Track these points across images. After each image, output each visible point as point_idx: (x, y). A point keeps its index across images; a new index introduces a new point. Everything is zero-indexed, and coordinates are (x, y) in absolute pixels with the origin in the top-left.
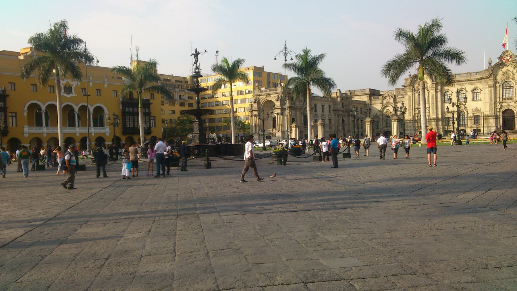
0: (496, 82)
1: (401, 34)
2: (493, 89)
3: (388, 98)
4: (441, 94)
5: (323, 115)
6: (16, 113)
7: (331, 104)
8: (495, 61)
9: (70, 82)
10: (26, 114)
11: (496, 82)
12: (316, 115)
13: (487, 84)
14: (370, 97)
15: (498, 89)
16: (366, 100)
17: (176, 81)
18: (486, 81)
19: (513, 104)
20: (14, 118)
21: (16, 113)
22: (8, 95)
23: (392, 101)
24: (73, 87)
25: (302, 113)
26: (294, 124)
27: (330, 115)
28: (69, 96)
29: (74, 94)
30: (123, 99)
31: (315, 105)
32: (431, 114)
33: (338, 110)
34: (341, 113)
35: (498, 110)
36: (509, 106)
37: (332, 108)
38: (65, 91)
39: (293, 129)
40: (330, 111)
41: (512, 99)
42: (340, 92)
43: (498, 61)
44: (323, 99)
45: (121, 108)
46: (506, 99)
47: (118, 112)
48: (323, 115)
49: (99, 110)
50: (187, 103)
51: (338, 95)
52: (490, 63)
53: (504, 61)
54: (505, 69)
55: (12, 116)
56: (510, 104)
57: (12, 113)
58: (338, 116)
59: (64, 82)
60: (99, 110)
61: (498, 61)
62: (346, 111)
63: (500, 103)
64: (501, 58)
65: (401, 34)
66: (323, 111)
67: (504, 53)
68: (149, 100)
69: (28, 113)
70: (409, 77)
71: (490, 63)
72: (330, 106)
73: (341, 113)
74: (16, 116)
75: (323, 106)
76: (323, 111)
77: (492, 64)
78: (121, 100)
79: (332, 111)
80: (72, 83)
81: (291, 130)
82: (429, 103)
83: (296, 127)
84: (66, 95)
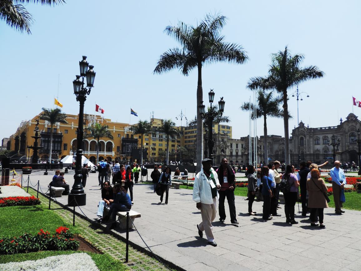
1: (43, 109)
5: (237, 149)
8: (344, 120)
10: (71, 145)
30: (123, 138)
31: (231, 144)
32: (307, 151)
36: (353, 148)
37: (244, 146)
43: (346, 120)
45: (122, 143)
47: (119, 145)
48: (237, 149)
49: (109, 144)
52: (341, 120)
53: (350, 120)
54: (350, 125)
56: (355, 147)
60: (109, 144)
61: (346, 120)
64: (348, 118)
65: (43, 109)
66: (237, 147)
68: (137, 139)
69: (73, 144)
72: (242, 145)
75: (237, 145)
76: (237, 147)
77: (343, 122)
78: (122, 139)
82: (306, 145)
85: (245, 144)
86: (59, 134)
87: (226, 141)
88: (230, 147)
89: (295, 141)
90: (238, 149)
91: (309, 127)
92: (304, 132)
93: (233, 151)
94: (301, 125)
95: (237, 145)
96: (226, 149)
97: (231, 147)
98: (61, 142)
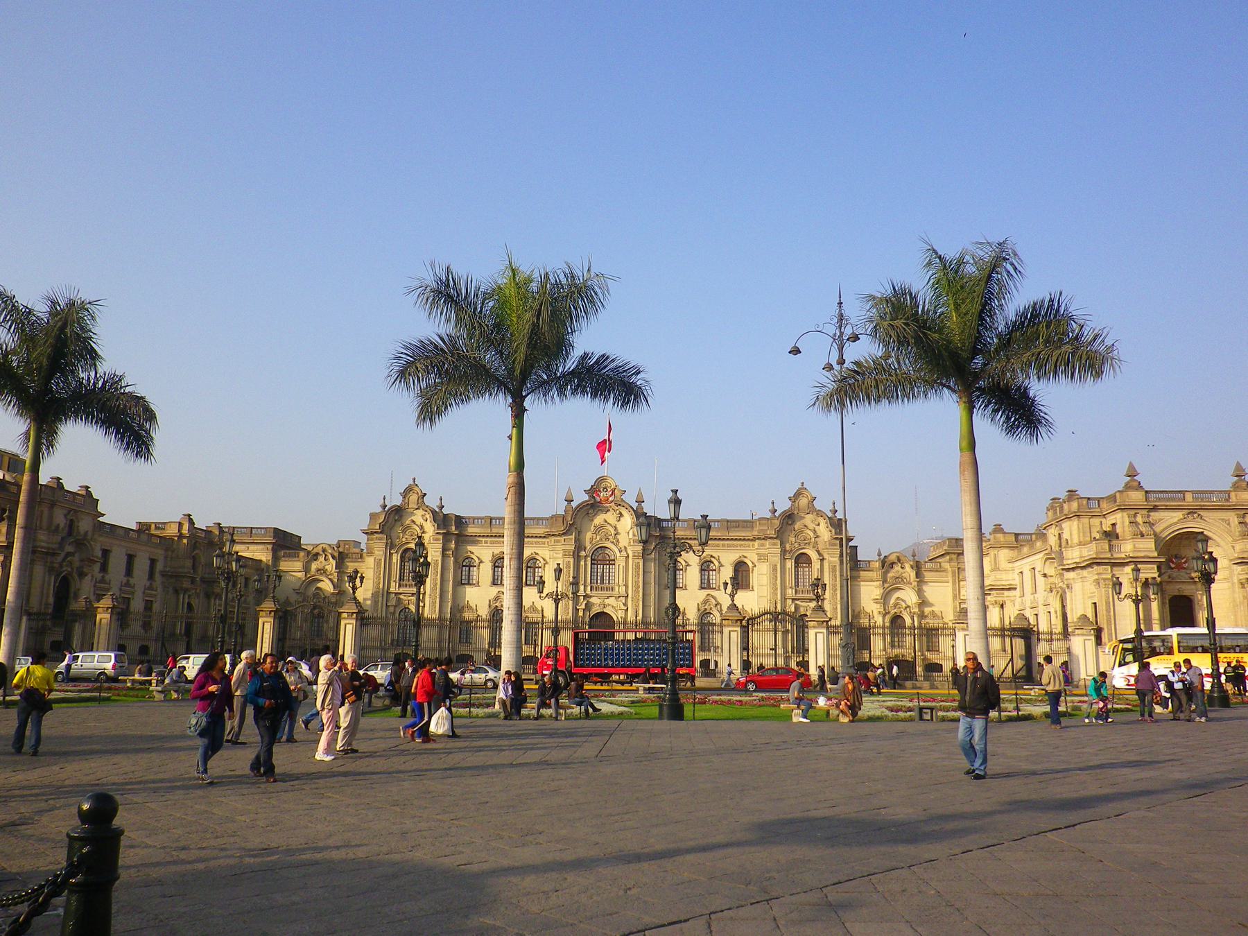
0: (579, 546)
2: (572, 561)
3: (321, 559)
4: (456, 561)
5: (127, 584)
7: (159, 554)
8: (580, 498)
11: (579, 546)
12: (103, 581)
13: (558, 548)
14: (274, 551)
15: (582, 563)
16: (264, 559)
18: (558, 541)
19: (612, 601)
23: (331, 566)
25: (51, 570)
27: (151, 588)
31: (106, 553)
33: (177, 576)
34: (186, 584)
35: (581, 614)
37: (159, 566)
40: (151, 576)
41: (612, 589)
42: (191, 522)
43: (586, 497)
44: (135, 535)
46: (598, 589)
48: (127, 584)
51: (185, 530)
52: (570, 501)
56: (607, 601)
58: (176, 592)
61: (586, 497)
62: (203, 580)
63: (586, 596)
64: (593, 491)
66: (129, 572)
67: (600, 480)
70: (380, 509)
71: (570, 501)
72: (153, 562)
73: (186, 584)
75: (130, 558)
76: (129, 572)
77: (574, 504)
79: (158, 577)
85: (166, 557)
87: (86, 533)
88: (97, 567)
89: (378, 563)
90: (132, 581)
91: (445, 511)
92: (422, 527)
93: (133, 593)
94: (413, 498)
95: (130, 558)
96: (82, 575)
97: (104, 568)
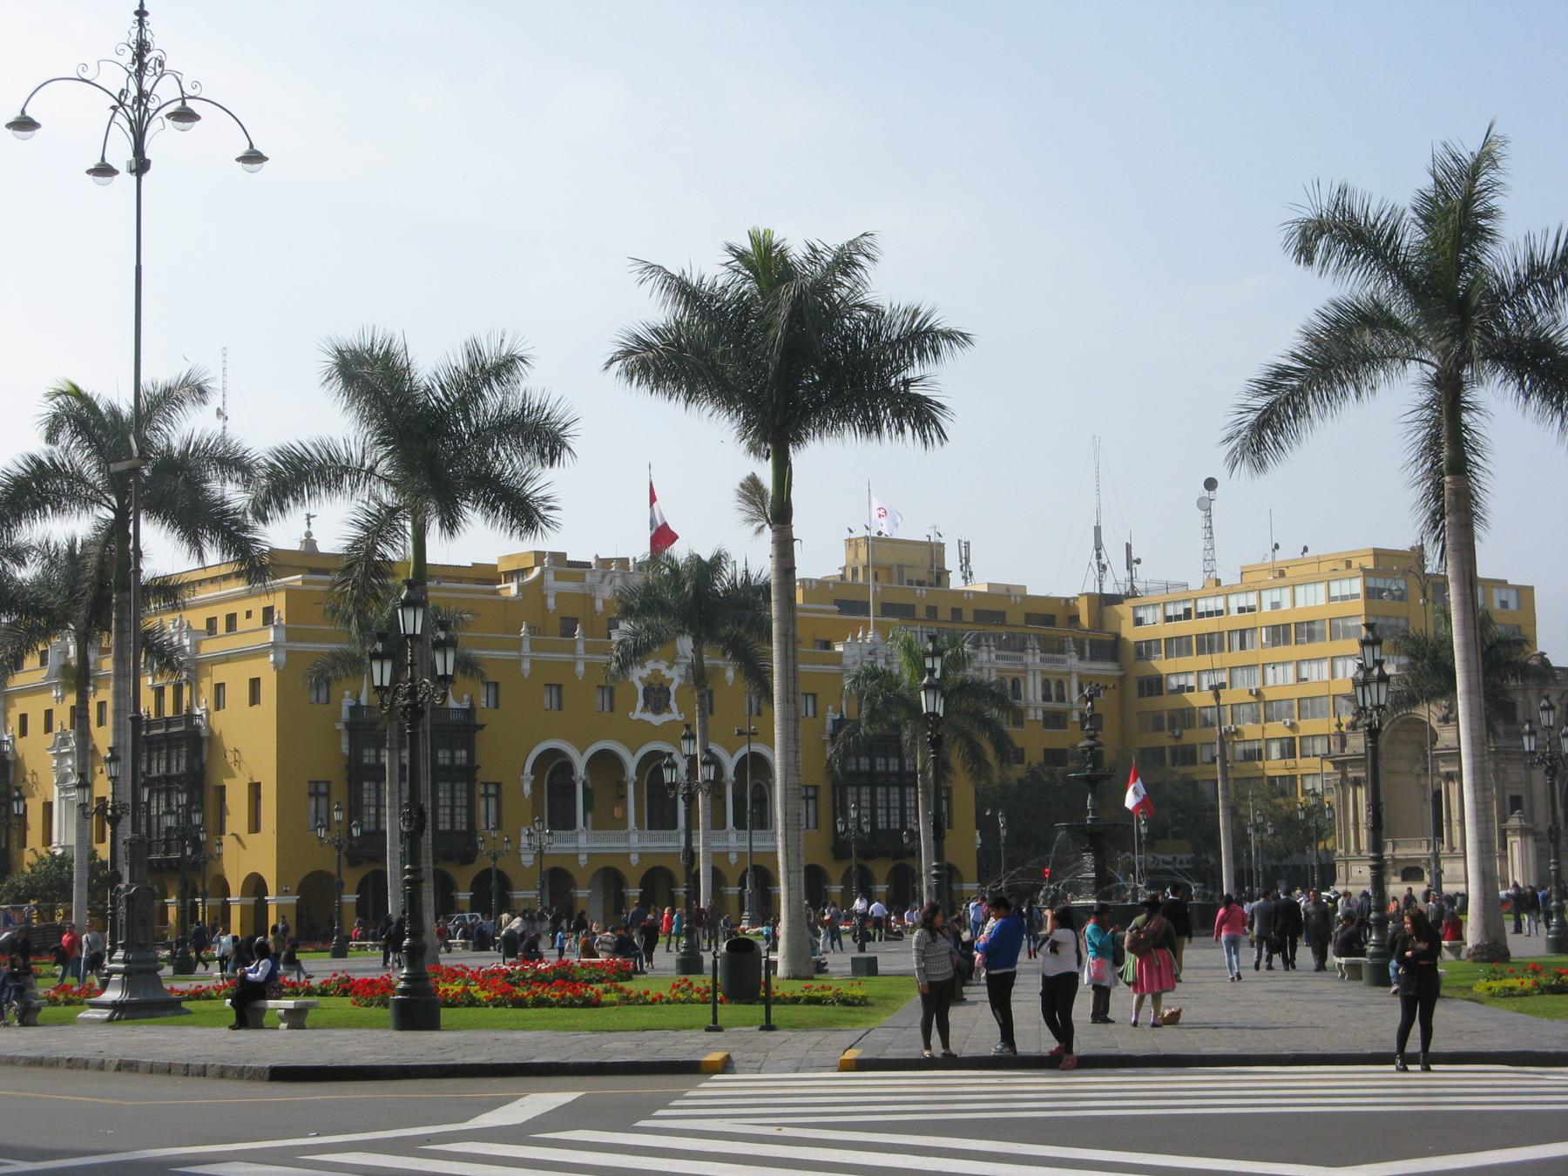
6: (498, 785)
9: (665, 672)
10: (527, 788)
17: (1031, 618)
20: (492, 801)
21: (498, 785)
22: (482, 727)
24: (673, 689)
26: (1514, 822)
28: (657, 720)
29: (674, 714)
38: (646, 704)
39: (1515, 845)
50: (1076, 716)
55: (487, 796)
57: (486, 785)
59: (645, 673)
69: (533, 786)
74: (498, 796)
80: (668, 674)
81: (1504, 846)
83: (1524, 832)
84: (649, 717)
86: (453, 717)
98: (467, 774)
